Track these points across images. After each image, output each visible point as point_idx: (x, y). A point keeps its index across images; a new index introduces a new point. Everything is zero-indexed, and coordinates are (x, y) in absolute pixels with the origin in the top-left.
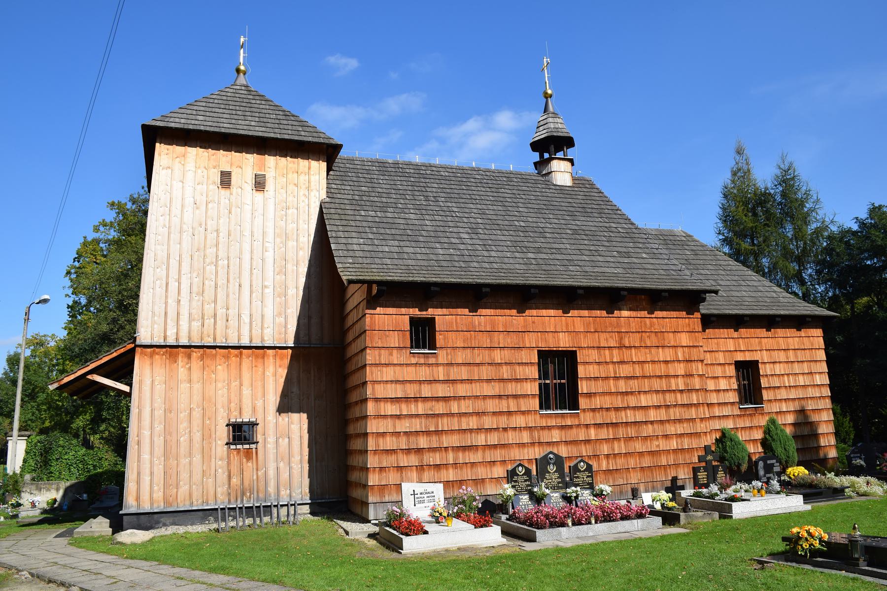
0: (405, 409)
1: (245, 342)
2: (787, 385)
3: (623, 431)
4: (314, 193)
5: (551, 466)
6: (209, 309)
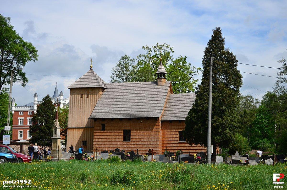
0: (99, 140)
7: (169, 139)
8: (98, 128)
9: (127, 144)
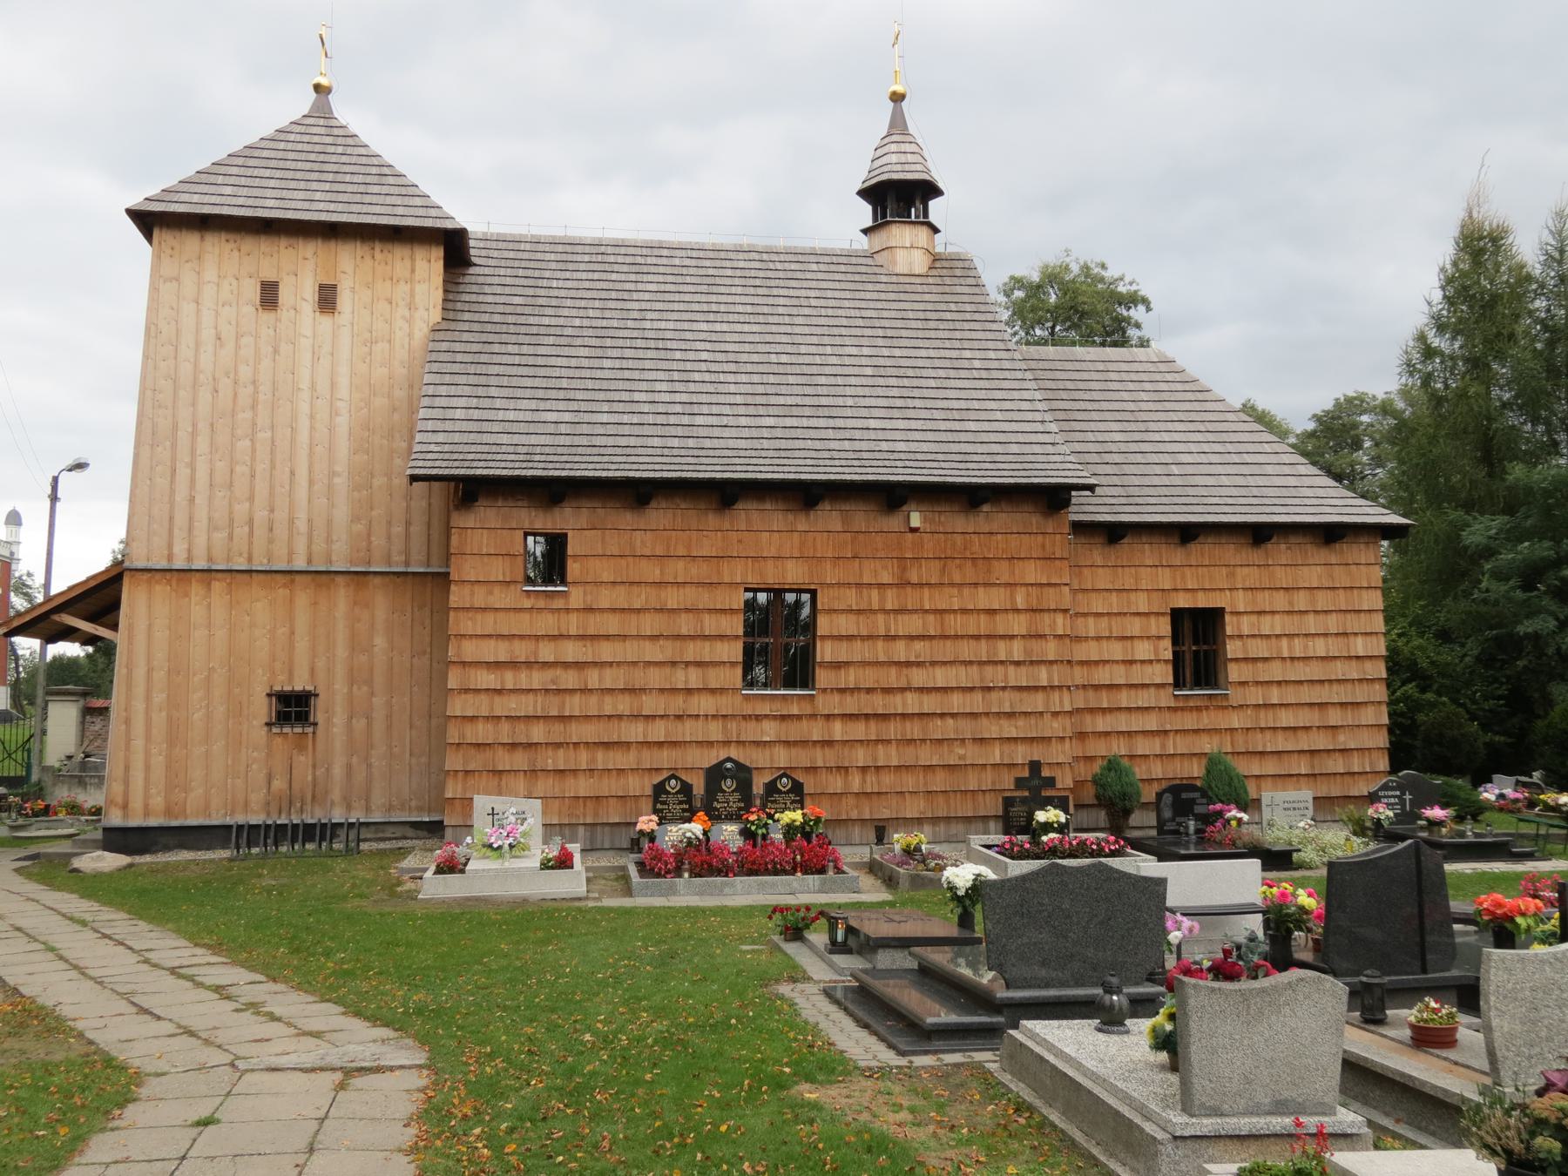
1: (300, 564)
2: (1286, 654)
3: (896, 728)
4: (420, 314)
5: (729, 782)
6: (241, 509)
7: (1102, 676)
8: (498, 570)
9: (783, 718)
